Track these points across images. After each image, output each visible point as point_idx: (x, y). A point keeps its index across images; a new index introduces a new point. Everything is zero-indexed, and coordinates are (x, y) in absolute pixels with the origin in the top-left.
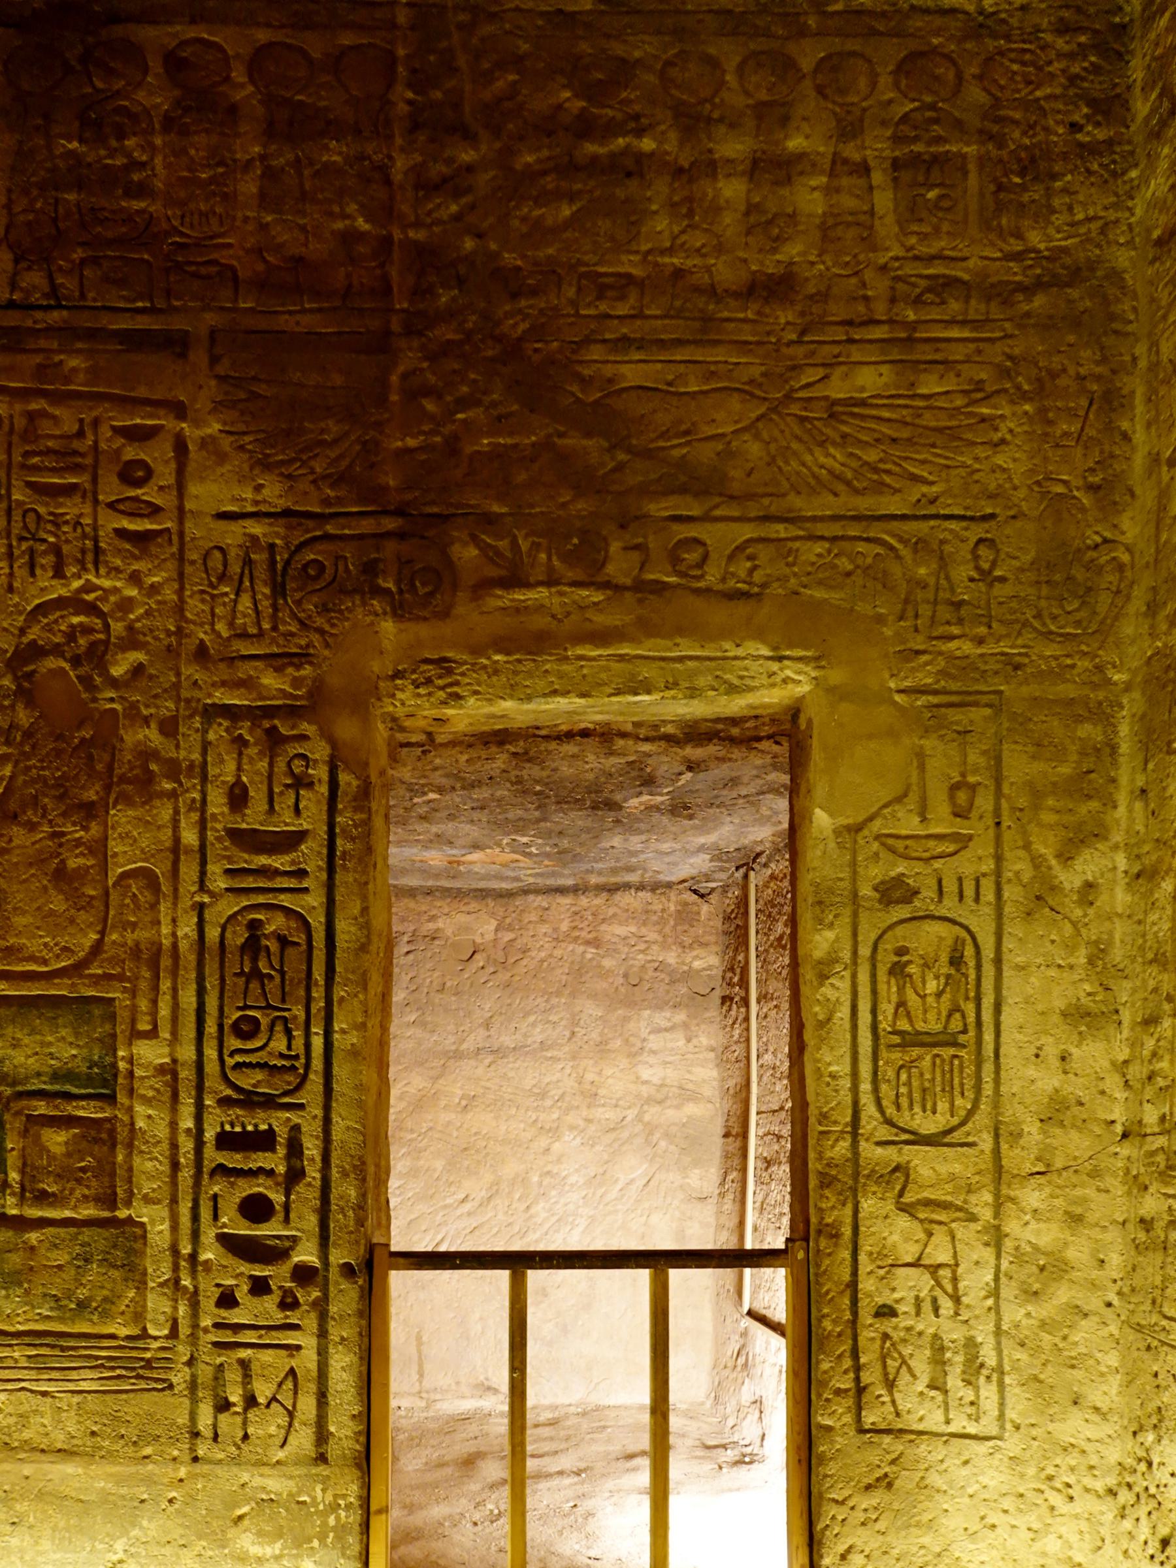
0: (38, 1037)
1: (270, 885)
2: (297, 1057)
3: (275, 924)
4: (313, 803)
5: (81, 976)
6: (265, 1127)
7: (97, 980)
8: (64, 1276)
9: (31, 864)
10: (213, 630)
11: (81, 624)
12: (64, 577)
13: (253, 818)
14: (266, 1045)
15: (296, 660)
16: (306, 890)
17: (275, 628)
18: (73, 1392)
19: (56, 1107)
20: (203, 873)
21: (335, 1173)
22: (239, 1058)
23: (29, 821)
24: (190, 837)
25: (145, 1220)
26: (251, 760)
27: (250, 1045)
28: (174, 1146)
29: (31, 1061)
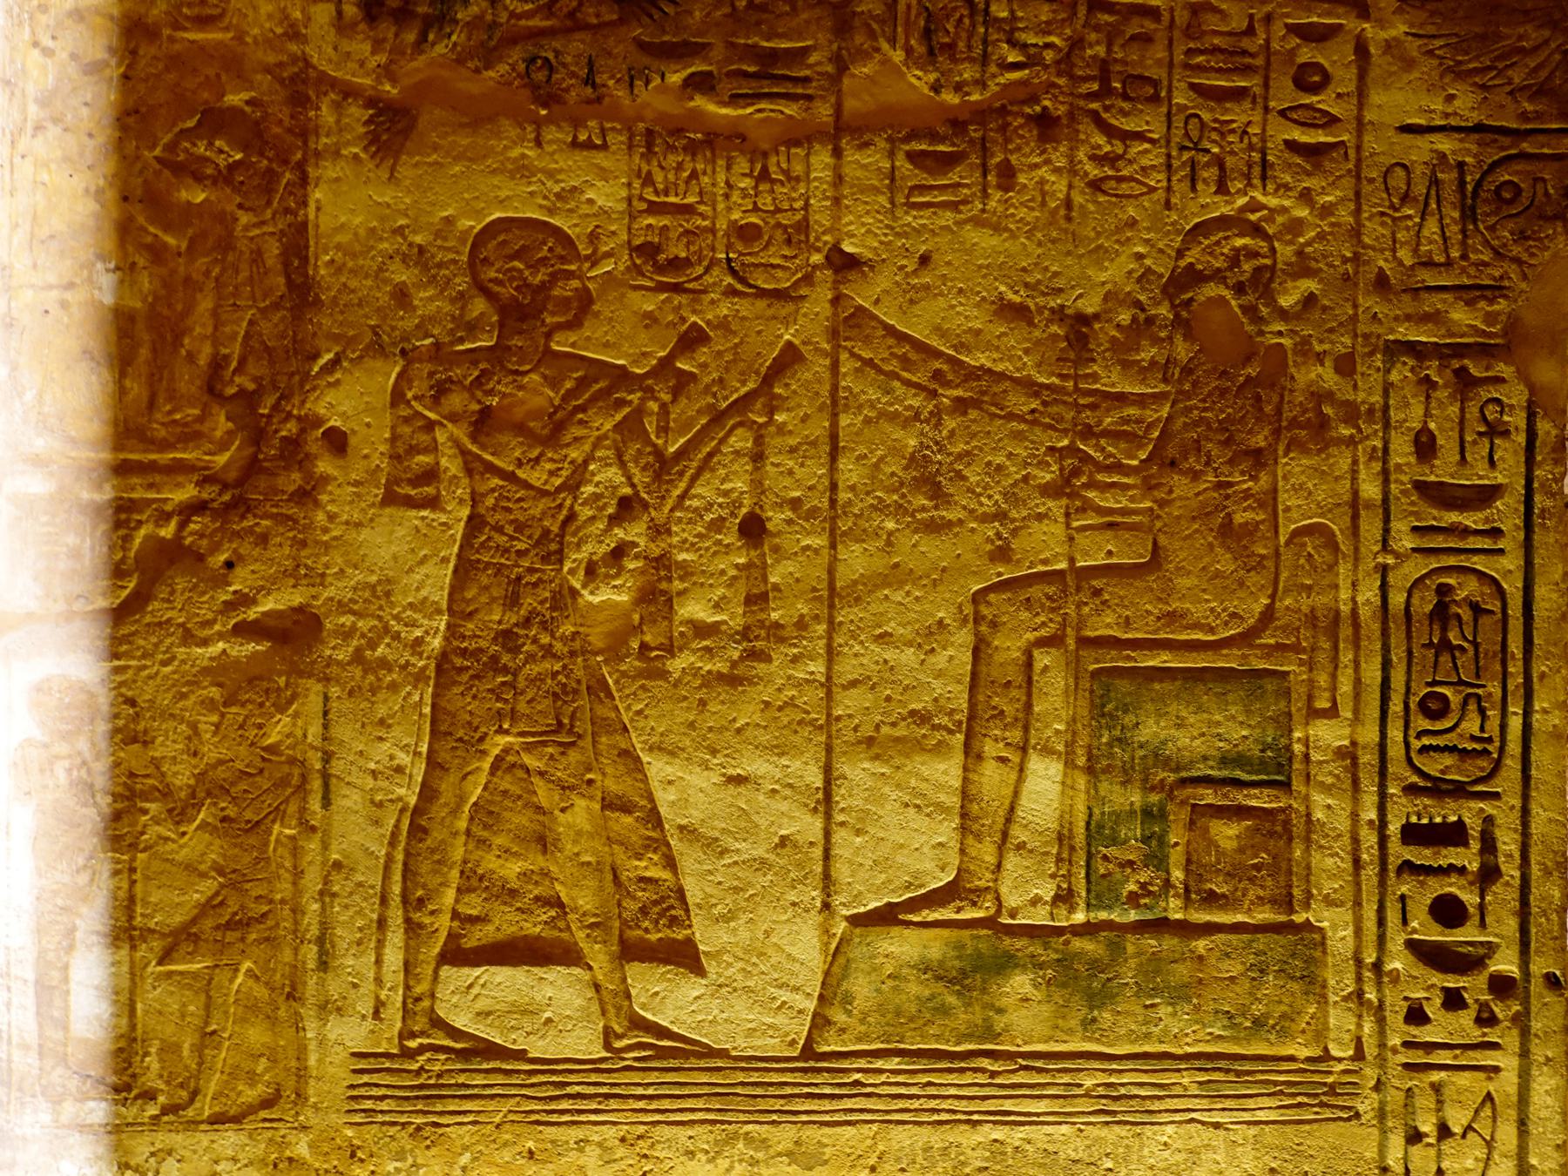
0: (1205, 715)
1: (1461, 545)
2: (1490, 740)
3: (1467, 589)
4: (1510, 453)
5: (1251, 646)
8: (1238, 989)
9: (1194, 518)
10: (1395, 257)
11: (1245, 247)
12: (1228, 193)
13: (1443, 471)
14: (1456, 725)
15: (1489, 293)
16: (1501, 551)
17: (1464, 257)
18: (1248, 1123)
19: (1225, 796)
20: (1386, 531)
21: (1535, 871)
22: (1426, 741)
23: (1191, 469)
24: (1370, 490)
25: (1325, 924)
26: (1441, 404)
27: (1439, 726)
28: (1356, 840)
29: (1198, 742)
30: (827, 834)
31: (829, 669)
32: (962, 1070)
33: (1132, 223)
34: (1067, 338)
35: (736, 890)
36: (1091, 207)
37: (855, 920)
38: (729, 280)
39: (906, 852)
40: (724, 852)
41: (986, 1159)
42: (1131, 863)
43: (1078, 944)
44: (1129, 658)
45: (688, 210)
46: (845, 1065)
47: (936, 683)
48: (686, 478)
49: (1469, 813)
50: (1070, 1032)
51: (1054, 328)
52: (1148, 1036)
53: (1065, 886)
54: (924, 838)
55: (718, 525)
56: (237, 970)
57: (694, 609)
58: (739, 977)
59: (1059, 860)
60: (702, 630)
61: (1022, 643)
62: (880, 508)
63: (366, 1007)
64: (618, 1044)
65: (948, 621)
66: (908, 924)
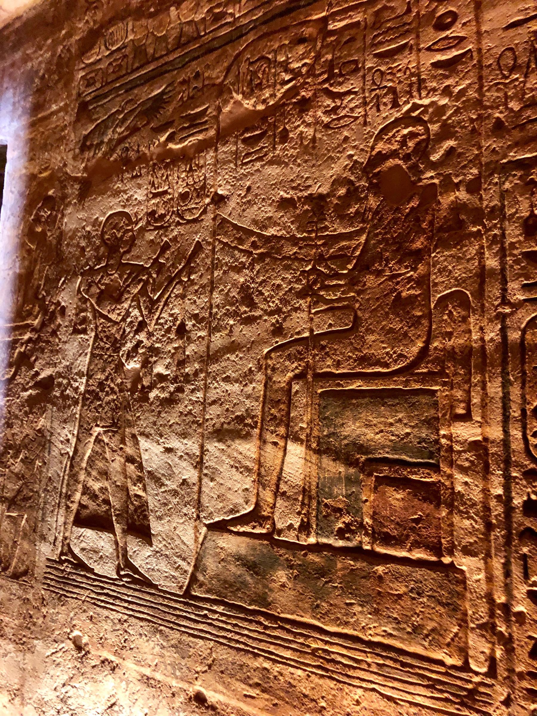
0: (383, 419)
5: (413, 374)
8: (402, 603)
10: (507, 108)
12: (399, 106)
18: (410, 703)
19: (396, 471)
23: (377, 270)
25: (464, 568)
28: (487, 509)
29: (379, 436)
30: (200, 480)
31: (205, 395)
32: (251, 621)
33: (346, 139)
34: (312, 210)
35: (165, 504)
36: (325, 138)
37: (210, 527)
38: (177, 219)
39: (231, 492)
40: (163, 485)
41: (260, 679)
42: (339, 510)
43: (312, 557)
44: (339, 385)
45: (165, 192)
46: (201, 604)
47: (247, 402)
48: (159, 311)
50: (304, 610)
51: (306, 207)
52: (347, 623)
53: (305, 520)
54: (239, 485)
55: (168, 330)
57: (160, 369)
58: (163, 549)
59: (303, 504)
60: (161, 378)
61: (286, 378)
62: (228, 314)
63: (51, 539)
64: (122, 573)
66: (231, 532)
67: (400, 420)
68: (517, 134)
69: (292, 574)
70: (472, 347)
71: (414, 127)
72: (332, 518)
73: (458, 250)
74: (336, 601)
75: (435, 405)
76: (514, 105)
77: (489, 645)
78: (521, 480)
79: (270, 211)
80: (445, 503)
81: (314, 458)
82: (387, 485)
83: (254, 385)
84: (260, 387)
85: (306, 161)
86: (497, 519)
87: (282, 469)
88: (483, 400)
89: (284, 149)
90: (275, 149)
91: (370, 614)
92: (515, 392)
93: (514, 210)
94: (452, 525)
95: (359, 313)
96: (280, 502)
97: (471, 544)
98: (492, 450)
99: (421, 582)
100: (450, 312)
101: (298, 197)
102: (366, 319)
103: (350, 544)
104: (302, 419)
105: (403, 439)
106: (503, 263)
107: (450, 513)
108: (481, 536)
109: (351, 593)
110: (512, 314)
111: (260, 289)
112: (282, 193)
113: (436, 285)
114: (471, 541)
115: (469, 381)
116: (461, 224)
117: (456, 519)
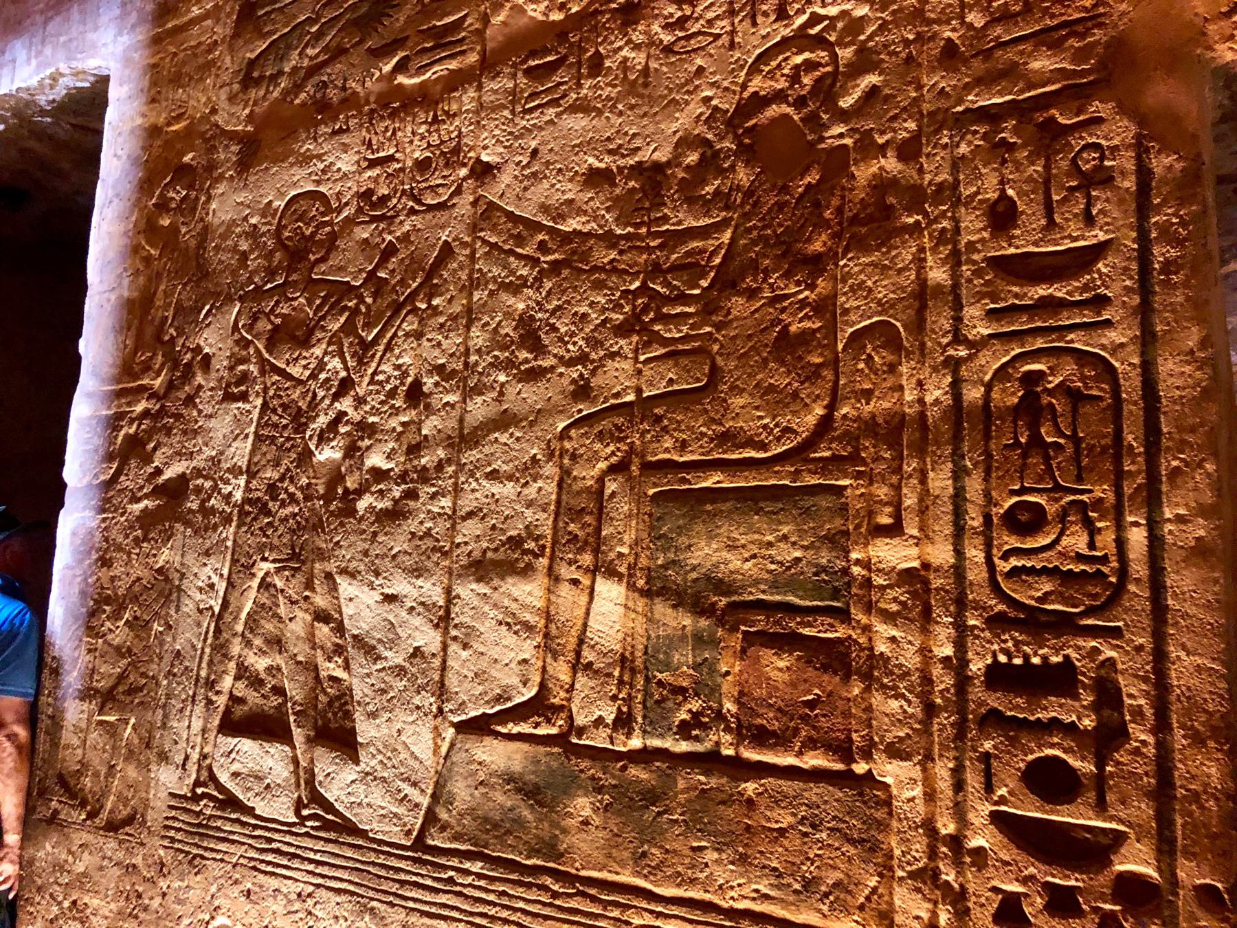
0: (756, 536)
2: (1104, 560)
6: (1059, 659)
7: (824, 466)
8: (786, 843)
10: (963, 22)
11: (806, 61)
12: (789, 17)
14: (1056, 542)
15: (1080, 29)
16: (1108, 323)
19: (777, 623)
20: (958, 319)
21: (1179, 739)
22: (1014, 562)
26: (1018, 166)
28: (927, 680)
29: (749, 565)
30: (445, 647)
31: (455, 504)
32: (529, 886)
33: (700, 70)
34: (642, 189)
35: (384, 691)
36: (665, 69)
37: (461, 727)
38: (411, 203)
39: (498, 666)
40: (379, 658)
42: (682, 691)
43: (636, 772)
45: (391, 158)
46: (443, 861)
47: (528, 513)
48: (376, 360)
49: (1075, 650)
51: (632, 184)
52: (693, 881)
53: (625, 709)
54: (512, 654)
55: (392, 394)
56: (127, 724)
57: (376, 459)
58: (379, 768)
59: (621, 682)
60: (379, 475)
61: (595, 472)
62: (496, 365)
63: (179, 759)
64: (305, 812)
65: (539, 457)
66: (497, 734)
67: (785, 538)
68: (978, 66)
69: (601, 802)
70: (904, 415)
71: (812, 52)
72: (670, 704)
73: (884, 254)
74: (676, 845)
75: (844, 508)
76: (976, 19)
77: (930, 906)
78: (983, 630)
79: (571, 191)
80: (858, 673)
81: (641, 603)
82: (762, 645)
83: (540, 483)
84: (551, 487)
85: (632, 107)
86: (943, 697)
87: (585, 625)
88: (921, 500)
89: (596, 87)
90: (579, 86)
91: (733, 863)
92: (974, 486)
93: (975, 189)
94: (869, 709)
95: (720, 361)
96: (582, 681)
97: (901, 739)
98: (937, 583)
99: (818, 807)
100: (870, 356)
101: (618, 167)
102: (730, 371)
103: (699, 748)
104: (621, 540)
105: (789, 568)
106: (955, 275)
107: (868, 689)
108: (917, 726)
109: (699, 830)
110: (970, 358)
111: (552, 321)
112: (591, 160)
113: (846, 312)
114: (901, 734)
115: (898, 470)
116: (888, 212)
117: (877, 699)
